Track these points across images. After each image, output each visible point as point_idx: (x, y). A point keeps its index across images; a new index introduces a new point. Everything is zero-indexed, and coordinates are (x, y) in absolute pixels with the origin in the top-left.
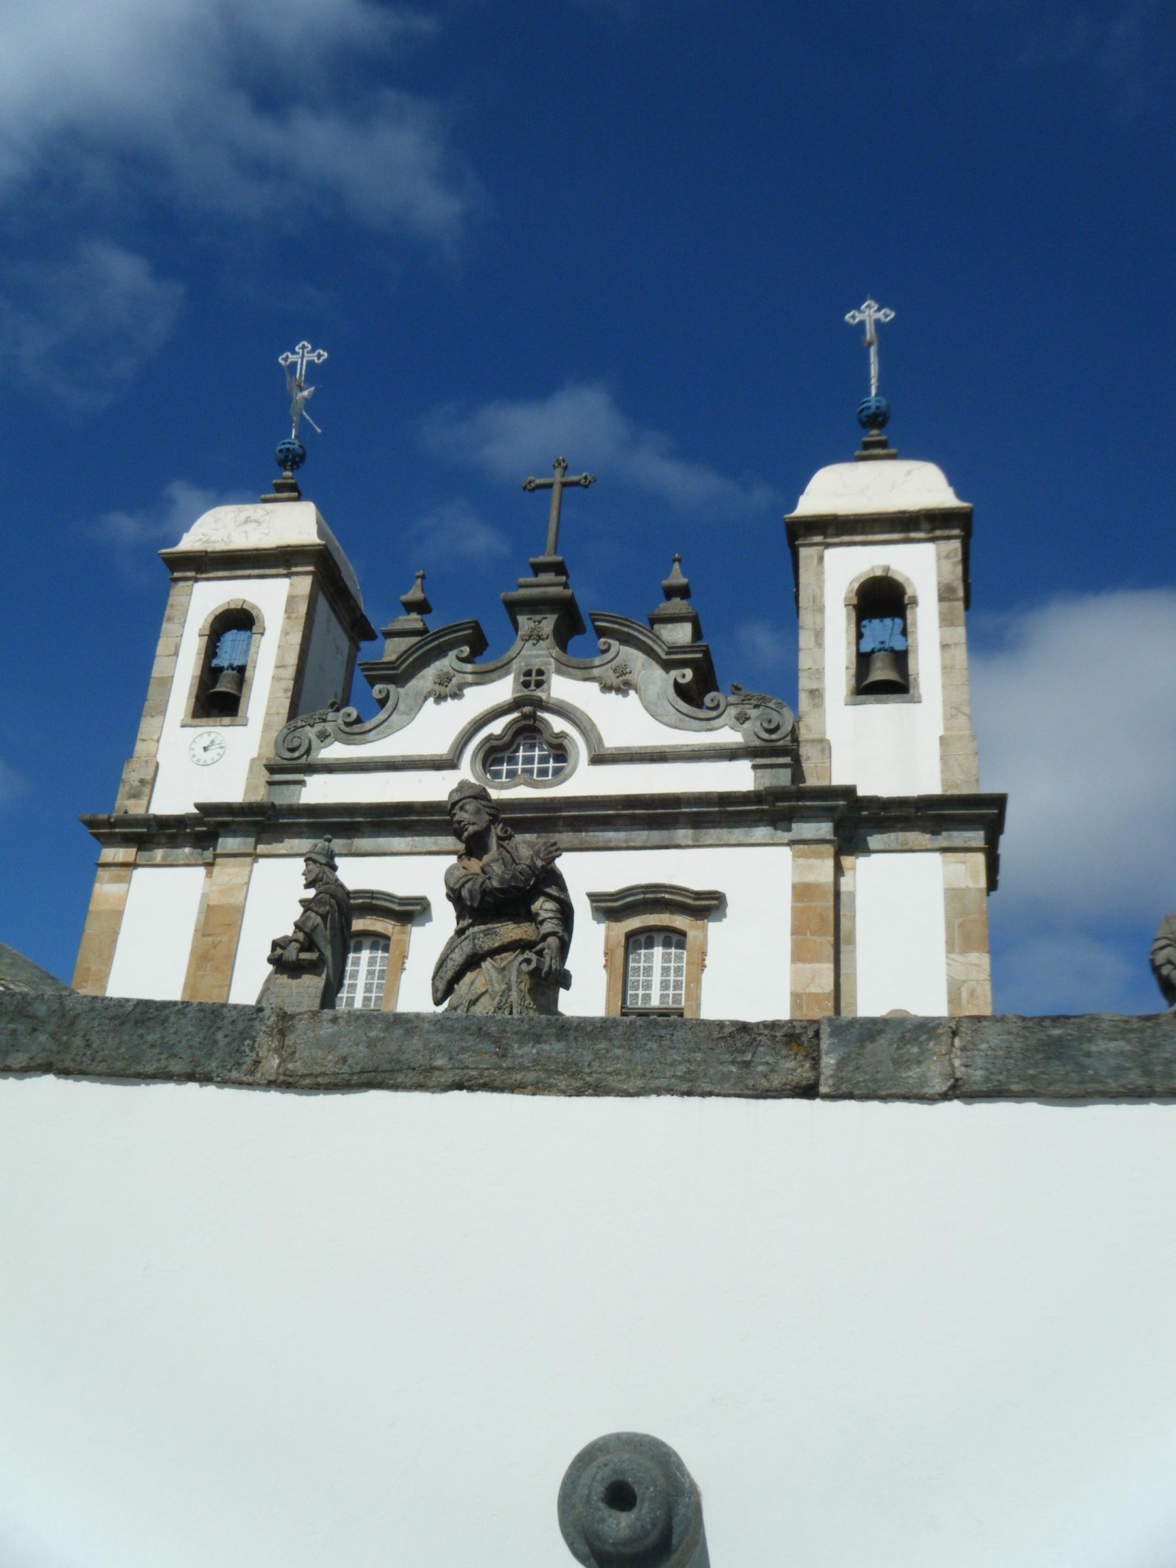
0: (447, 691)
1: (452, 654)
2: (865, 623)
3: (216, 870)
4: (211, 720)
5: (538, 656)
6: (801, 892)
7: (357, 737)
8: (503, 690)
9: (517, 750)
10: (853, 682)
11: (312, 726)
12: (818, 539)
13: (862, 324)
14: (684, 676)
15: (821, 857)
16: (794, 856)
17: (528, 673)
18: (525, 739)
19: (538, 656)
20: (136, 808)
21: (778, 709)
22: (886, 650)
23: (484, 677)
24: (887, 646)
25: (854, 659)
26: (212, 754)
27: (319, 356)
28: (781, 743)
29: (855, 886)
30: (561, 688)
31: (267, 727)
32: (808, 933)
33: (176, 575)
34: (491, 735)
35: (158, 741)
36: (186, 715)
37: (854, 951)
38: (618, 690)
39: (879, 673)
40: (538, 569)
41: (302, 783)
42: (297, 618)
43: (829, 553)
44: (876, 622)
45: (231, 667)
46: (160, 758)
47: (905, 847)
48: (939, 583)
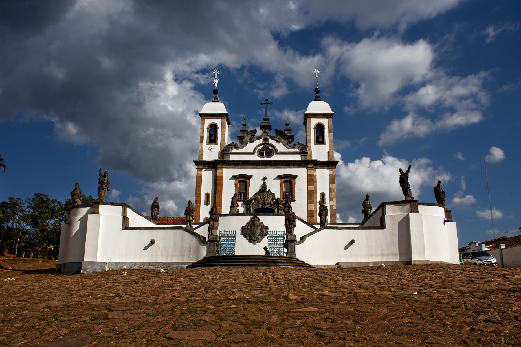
0: (252, 141)
3: (218, 170)
4: (212, 144)
8: (261, 141)
13: (315, 73)
17: (265, 138)
23: (258, 138)
30: (271, 141)
34: (260, 149)
38: (279, 142)
40: (265, 119)
43: (311, 119)
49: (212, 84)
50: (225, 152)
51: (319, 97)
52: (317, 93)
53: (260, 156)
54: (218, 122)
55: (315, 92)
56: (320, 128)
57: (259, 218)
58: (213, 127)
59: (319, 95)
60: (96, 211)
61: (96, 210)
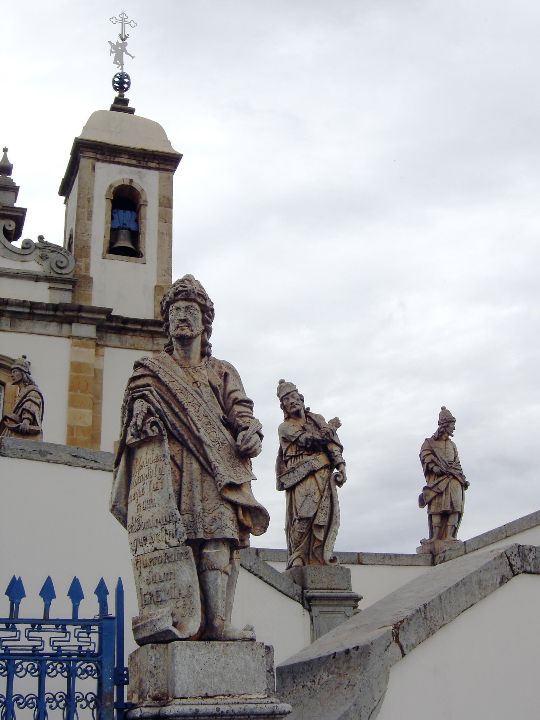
2: (115, 211)
6: (76, 367)
10: (108, 245)
14: (10, 226)
15: (88, 348)
16: (72, 345)
21: (66, 255)
22: (126, 229)
24: (127, 226)
25: (109, 231)
29: (103, 366)
32: (79, 391)
37: (101, 404)
39: (122, 242)
44: (121, 212)
47: (132, 347)
51: (126, 102)
55: (114, 82)
59: (127, 95)
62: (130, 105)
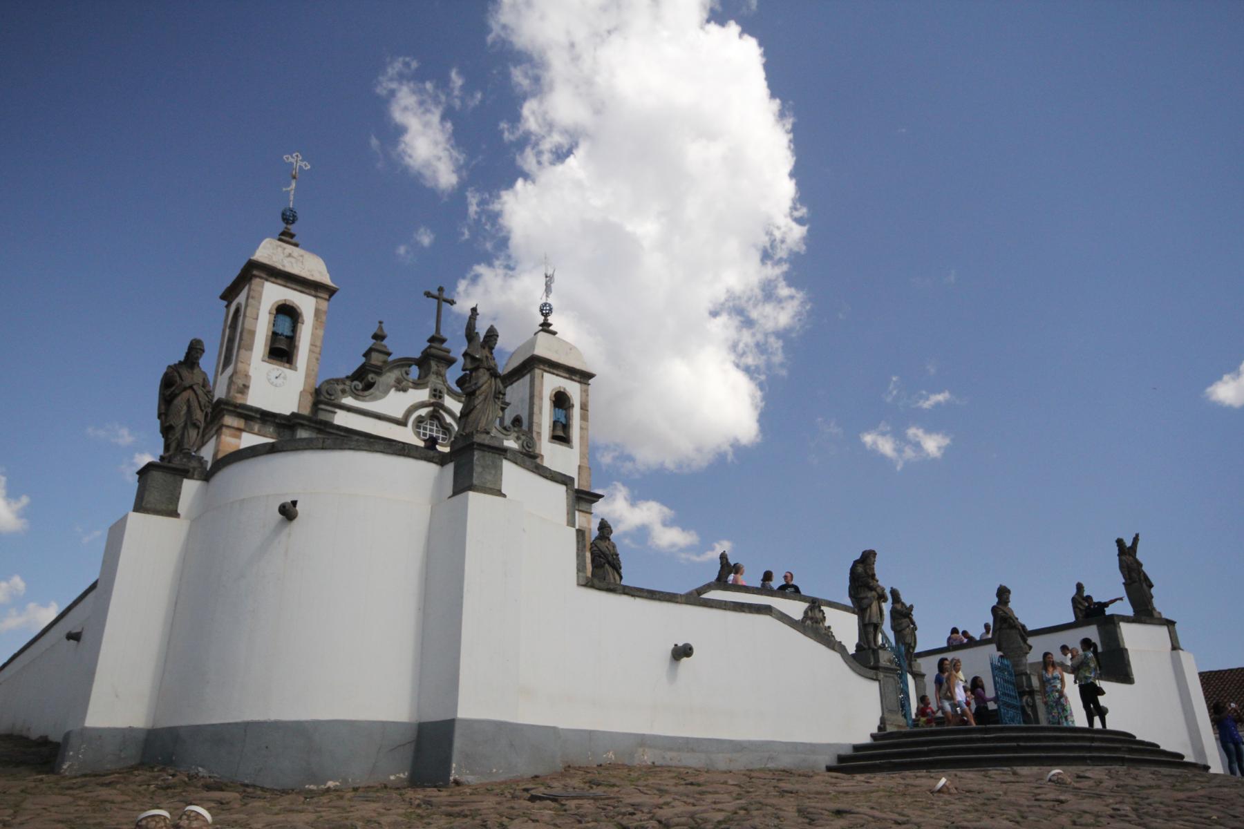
0: (401, 387)
1: (404, 370)
5: (439, 383)
7: (360, 397)
8: (423, 395)
9: (426, 424)
10: (551, 433)
11: (338, 384)
12: (542, 367)
17: (435, 390)
18: (430, 420)
19: (439, 383)
20: (239, 400)
23: (418, 385)
26: (279, 381)
27: (306, 166)
28: (532, 454)
31: (307, 376)
33: (255, 272)
34: (420, 416)
35: (249, 365)
36: (264, 356)
41: (335, 413)
42: (321, 322)
43: (546, 375)
44: (557, 409)
45: (282, 335)
46: (250, 374)
48: (581, 402)
49: (284, 189)
50: (322, 397)
51: (550, 325)
52: (546, 315)
53: (418, 434)
54: (306, 304)
56: (561, 400)
57: (824, 614)
58: (287, 311)
60: (488, 485)
61: (489, 477)
62: (551, 328)
